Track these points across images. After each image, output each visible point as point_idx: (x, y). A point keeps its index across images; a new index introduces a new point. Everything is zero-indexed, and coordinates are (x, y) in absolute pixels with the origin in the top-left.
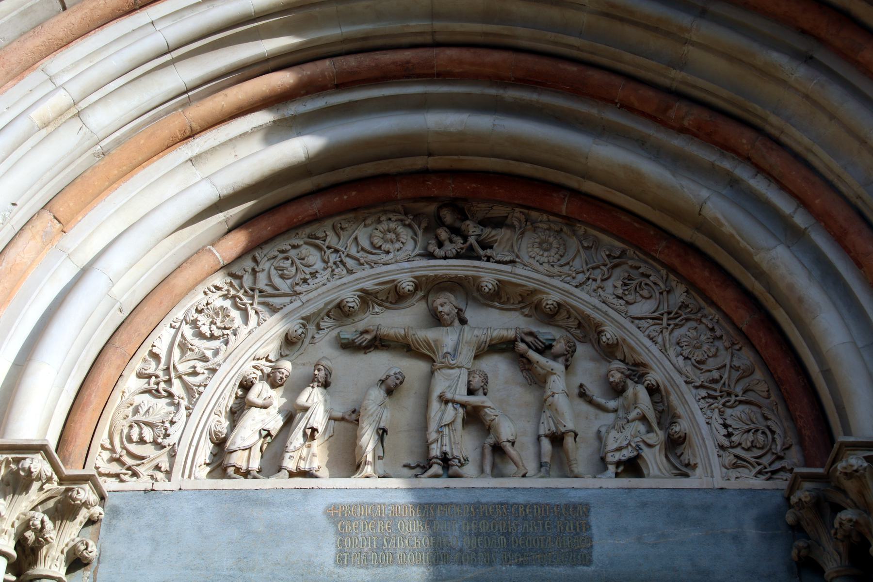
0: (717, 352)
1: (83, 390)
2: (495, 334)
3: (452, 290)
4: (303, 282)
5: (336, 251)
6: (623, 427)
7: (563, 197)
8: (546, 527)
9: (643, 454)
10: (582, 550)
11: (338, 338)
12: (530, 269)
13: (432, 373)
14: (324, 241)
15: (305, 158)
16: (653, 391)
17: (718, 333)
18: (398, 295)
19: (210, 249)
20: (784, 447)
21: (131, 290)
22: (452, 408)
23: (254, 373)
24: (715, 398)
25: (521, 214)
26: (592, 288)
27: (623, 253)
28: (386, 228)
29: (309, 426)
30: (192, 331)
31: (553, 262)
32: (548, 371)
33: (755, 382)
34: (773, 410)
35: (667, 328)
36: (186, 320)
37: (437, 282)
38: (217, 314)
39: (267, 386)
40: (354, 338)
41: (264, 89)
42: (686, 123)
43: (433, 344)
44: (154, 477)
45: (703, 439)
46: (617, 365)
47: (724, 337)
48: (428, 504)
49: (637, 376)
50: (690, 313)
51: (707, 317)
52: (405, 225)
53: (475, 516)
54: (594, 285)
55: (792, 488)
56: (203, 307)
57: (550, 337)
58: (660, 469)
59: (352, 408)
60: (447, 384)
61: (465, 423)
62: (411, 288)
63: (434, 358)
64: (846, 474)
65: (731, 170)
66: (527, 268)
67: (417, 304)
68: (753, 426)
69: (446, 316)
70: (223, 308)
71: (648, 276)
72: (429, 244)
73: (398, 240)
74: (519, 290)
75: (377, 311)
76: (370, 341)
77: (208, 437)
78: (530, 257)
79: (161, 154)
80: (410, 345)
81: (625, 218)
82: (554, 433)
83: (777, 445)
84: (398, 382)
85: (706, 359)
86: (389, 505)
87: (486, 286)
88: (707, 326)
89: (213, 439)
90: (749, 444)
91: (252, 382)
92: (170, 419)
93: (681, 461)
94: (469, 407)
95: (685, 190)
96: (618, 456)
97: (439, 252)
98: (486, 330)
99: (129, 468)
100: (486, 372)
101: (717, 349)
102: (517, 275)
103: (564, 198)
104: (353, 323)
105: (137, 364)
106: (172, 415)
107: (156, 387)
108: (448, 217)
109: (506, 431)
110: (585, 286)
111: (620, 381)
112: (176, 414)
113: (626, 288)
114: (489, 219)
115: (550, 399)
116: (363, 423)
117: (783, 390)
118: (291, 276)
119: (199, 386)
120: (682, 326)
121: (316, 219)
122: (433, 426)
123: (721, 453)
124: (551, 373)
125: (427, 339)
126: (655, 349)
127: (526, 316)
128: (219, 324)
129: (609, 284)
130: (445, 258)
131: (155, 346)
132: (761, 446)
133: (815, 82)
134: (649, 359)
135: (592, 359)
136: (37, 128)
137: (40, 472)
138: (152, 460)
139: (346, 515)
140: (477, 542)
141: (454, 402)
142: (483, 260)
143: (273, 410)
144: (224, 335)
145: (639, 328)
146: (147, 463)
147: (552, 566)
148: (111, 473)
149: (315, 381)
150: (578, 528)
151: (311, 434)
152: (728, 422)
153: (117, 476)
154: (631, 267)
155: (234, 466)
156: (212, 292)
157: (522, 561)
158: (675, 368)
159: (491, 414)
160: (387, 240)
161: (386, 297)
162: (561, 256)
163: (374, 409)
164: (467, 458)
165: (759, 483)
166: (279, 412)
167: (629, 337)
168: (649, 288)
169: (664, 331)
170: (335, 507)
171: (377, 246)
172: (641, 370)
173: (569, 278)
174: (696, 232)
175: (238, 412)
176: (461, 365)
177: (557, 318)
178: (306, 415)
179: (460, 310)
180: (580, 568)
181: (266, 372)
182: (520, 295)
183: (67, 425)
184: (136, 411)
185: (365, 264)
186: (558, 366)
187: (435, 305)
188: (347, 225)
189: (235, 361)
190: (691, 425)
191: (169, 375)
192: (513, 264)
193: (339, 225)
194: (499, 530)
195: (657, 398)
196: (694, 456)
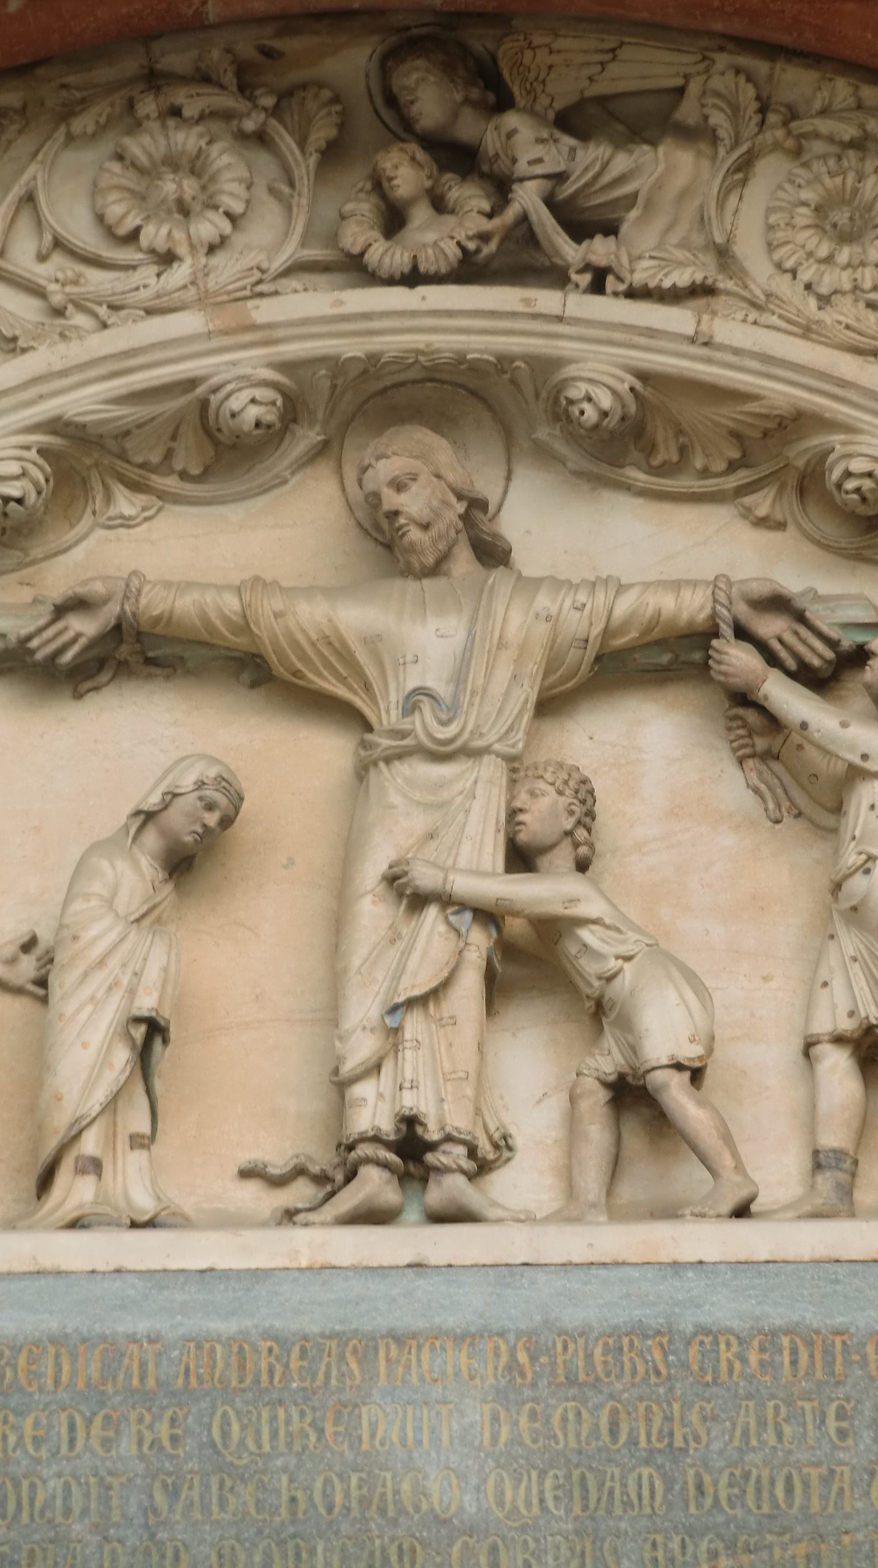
2: (623, 607)
8: (832, 1424)
12: (774, 320)
18: (216, 443)
22: (442, 928)
25: (742, 79)
37: (380, 385)
40: (24, 632)
43: (362, 657)
48: (333, 1335)
52: (242, 136)
60: (419, 822)
62: (270, 416)
67: (294, 481)
72: (343, 217)
75: (127, 510)
87: (589, 399)
100: (587, 773)
104: (21, 566)
114: (602, 100)
125: (337, 630)
140: (541, 1492)
163: (113, 936)
164: (505, 1138)
171: (123, 230)
176: (478, 743)
179: (477, 504)
182: (736, 436)
185: (70, 309)
192: (701, 302)
194: (633, 1442)
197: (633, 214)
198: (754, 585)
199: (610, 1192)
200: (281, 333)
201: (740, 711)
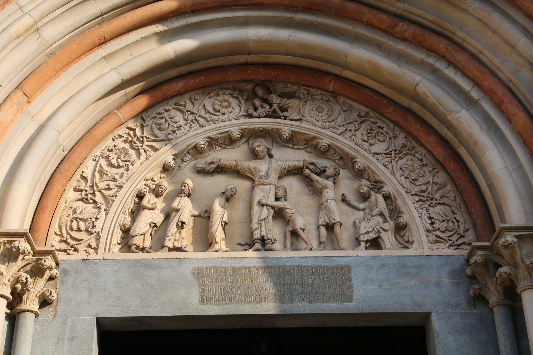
0: (424, 174)
1: (43, 199)
2: (291, 164)
3: (263, 137)
4: (173, 133)
5: (192, 113)
6: (369, 220)
7: (331, 80)
8: (325, 280)
9: (381, 236)
10: (347, 293)
11: (195, 166)
13: (253, 188)
14: (185, 107)
15: (174, 56)
16: (387, 197)
17: (425, 162)
19: (116, 113)
20: (465, 230)
21: (69, 138)
23: (145, 188)
24: (424, 201)
25: (305, 90)
26: (349, 135)
27: (367, 114)
28: (222, 99)
29: (180, 221)
30: (106, 163)
31: (325, 120)
32: (323, 186)
33: (447, 191)
34: (458, 208)
35: (394, 160)
36: (102, 156)
37: (255, 132)
38: (121, 152)
39: (153, 197)
40: (205, 167)
41: (149, 13)
42: (406, 35)
43: (253, 171)
44: (88, 252)
45: (417, 226)
46: (364, 182)
47: (429, 165)
49: (377, 188)
50: (408, 150)
51: (418, 153)
52: (234, 97)
53: (282, 274)
54: (350, 134)
55: (471, 254)
56: (112, 148)
57: (324, 166)
58: (391, 244)
59: (205, 210)
60: (263, 194)
61: (274, 218)
62: (239, 136)
63: (254, 179)
64: (504, 246)
65: (433, 64)
66: (309, 123)
67: (242, 146)
68: (446, 218)
69: (260, 153)
70: (124, 149)
71: (382, 128)
72: (248, 109)
73: (230, 106)
74: (304, 137)
75: (218, 150)
76: (215, 168)
77: (119, 227)
78: (311, 116)
79: (86, 54)
80: (239, 171)
81: (369, 93)
82: (328, 224)
83: (460, 229)
84: (233, 193)
85: (418, 178)
86: (230, 268)
87: (285, 134)
88: (418, 158)
89: (122, 228)
90: (444, 229)
91: (144, 194)
92: (95, 216)
93: (404, 239)
94: (276, 208)
95: (406, 76)
96: (367, 237)
97: (255, 114)
98: (285, 161)
99: (72, 247)
101: (424, 172)
102: (303, 127)
103: (331, 81)
105: (74, 183)
106: (96, 214)
107: (86, 197)
108: (260, 92)
109: (299, 223)
110: (344, 134)
111: (367, 192)
112: (99, 213)
113: (369, 135)
114: (285, 93)
115: (326, 203)
116: (213, 218)
117: (464, 196)
118: (166, 129)
119: (112, 196)
120: (403, 158)
121: (180, 94)
122: (255, 220)
123: (428, 234)
124: (325, 187)
125: (249, 167)
126: (387, 173)
127: (309, 152)
128: (122, 159)
129: (359, 133)
130: (259, 117)
131: (84, 172)
132: (451, 230)
133: (485, 11)
134: (384, 178)
135: (349, 179)
136: (13, 39)
137: (24, 249)
138: (86, 241)
139: (205, 274)
140: (284, 289)
141: (267, 205)
142: (282, 119)
143: (157, 211)
144: (126, 165)
145: (378, 160)
146: (83, 243)
147: (329, 302)
148: (61, 249)
149: (183, 193)
150: (344, 280)
151: (181, 225)
152: (432, 216)
153: (65, 251)
154: (372, 122)
155: (135, 245)
156: (117, 139)
157: (311, 300)
158: (400, 184)
159: (290, 212)
160: (223, 106)
161: (223, 141)
162: (330, 116)
164: (276, 239)
165: (450, 252)
166: (161, 212)
167: (372, 165)
168: (383, 135)
169: (393, 161)
170: (198, 269)
171: (217, 110)
172: (379, 185)
173: (334, 130)
174: (412, 101)
175: (136, 212)
176: (271, 183)
177: (328, 154)
178: (178, 214)
179: (269, 149)
180: (346, 303)
181: (151, 187)
182: (305, 140)
183: (34, 220)
184: (75, 212)
186: (329, 183)
187: (254, 146)
188: (198, 97)
189: (133, 181)
190: (410, 218)
191: (94, 190)
192: (300, 121)
193: (194, 97)
194: (297, 282)
195: (389, 202)
196: (412, 236)
197: (289, 109)
198: (309, 161)
199: (291, 247)
200: (241, 125)
201: (307, 179)
